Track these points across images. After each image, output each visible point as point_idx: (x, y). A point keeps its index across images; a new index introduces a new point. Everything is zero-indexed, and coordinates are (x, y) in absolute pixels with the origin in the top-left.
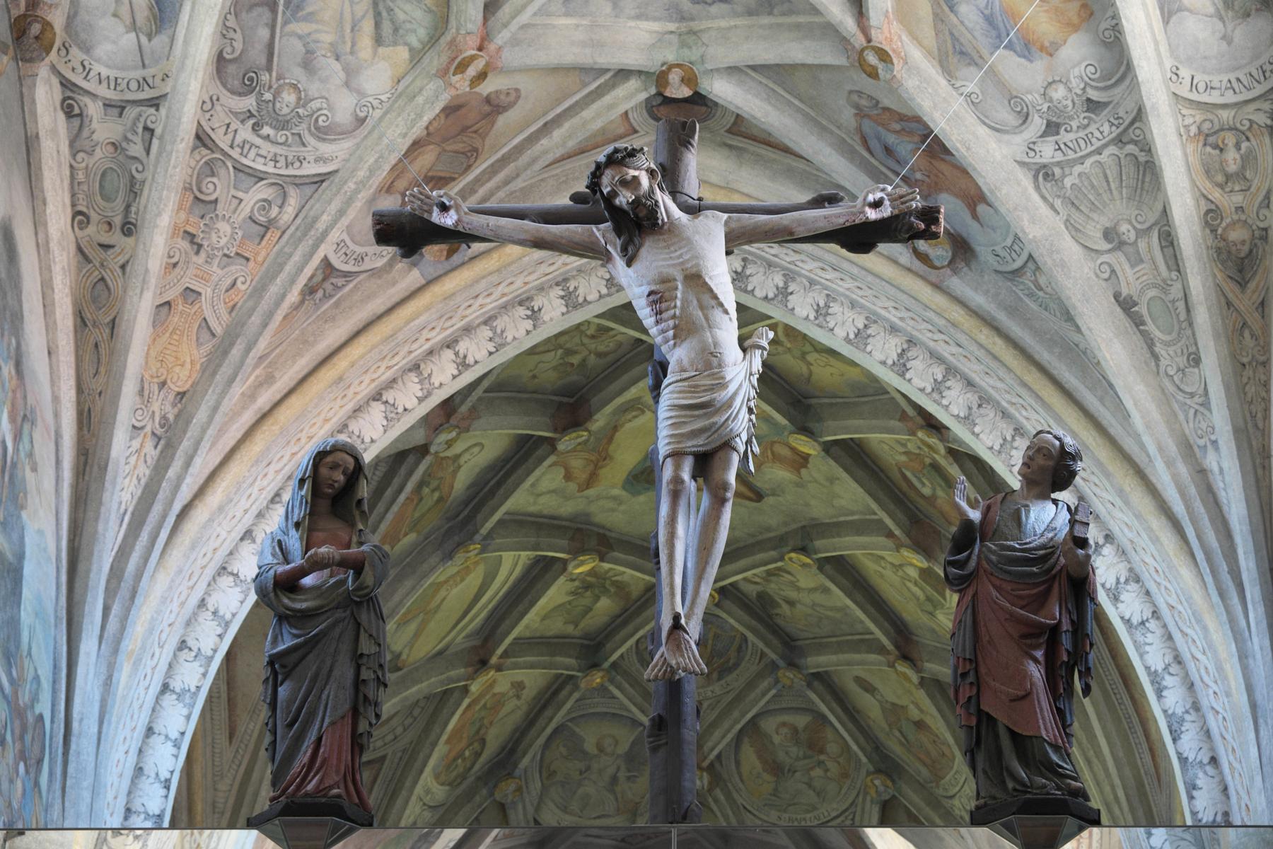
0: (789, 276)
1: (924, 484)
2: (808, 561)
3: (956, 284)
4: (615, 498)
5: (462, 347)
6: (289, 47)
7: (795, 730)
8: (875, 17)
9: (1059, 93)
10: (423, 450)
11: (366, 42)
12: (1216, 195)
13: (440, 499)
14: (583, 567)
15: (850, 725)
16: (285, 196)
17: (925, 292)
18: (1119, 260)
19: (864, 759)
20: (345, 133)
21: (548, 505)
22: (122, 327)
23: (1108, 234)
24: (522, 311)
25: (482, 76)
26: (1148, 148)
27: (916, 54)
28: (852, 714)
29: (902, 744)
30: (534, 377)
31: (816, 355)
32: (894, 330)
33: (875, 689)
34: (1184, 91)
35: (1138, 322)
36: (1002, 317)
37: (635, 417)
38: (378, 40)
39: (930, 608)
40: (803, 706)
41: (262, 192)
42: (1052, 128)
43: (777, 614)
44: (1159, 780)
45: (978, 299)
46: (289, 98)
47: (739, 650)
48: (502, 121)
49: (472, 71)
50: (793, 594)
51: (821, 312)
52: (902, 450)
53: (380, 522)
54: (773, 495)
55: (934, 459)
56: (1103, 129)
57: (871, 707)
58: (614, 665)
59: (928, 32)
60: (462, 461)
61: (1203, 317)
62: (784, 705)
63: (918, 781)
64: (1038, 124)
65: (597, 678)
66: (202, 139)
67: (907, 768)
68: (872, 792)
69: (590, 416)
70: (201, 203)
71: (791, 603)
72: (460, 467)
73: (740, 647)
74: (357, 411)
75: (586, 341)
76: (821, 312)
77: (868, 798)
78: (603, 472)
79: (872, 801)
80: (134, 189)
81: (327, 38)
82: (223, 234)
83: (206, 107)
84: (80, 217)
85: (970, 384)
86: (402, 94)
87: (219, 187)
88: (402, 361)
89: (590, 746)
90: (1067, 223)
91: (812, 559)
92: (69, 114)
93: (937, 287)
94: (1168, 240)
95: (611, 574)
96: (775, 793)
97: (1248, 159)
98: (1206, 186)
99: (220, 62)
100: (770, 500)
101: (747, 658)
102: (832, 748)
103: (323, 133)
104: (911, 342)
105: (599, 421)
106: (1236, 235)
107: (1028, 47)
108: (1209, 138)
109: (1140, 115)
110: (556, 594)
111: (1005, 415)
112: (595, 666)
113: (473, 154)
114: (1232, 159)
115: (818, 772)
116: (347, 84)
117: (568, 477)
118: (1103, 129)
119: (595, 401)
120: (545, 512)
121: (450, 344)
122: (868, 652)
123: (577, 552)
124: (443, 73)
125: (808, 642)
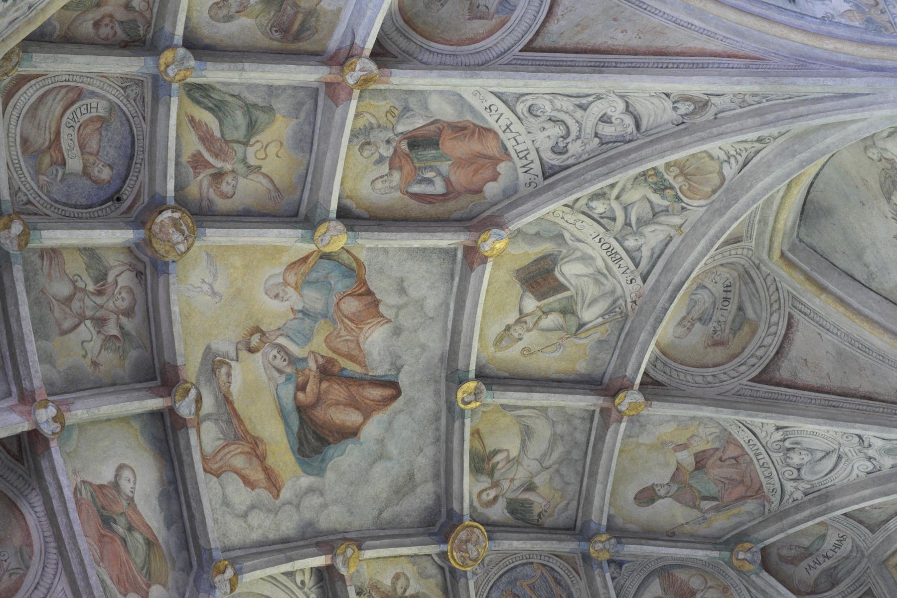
1: (430, 181)
2: (471, 385)
4: (311, 490)
13: (151, 543)
15: (680, 544)
19: (716, 554)
29: (717, 509)
30: (95, 364)
31: (250, 151)
33: (652, 488)
37: (229, 375)
39: (573, 322)
40: (643, 577)
43: (539, 515)
44: (759, 59)
47: (558, 583)
50: (521, 475)
52: (385, 168)
53: (71, 528)
54: (399, 370)
55: (406, 136)
60: (126, 487)
62: (633, 591)
63: (760, 522)
67: (744, 527)
68: (748, 567)
71: (530, 487)
72: (132, 499)
73: (555, 579)
75: (99, 300)
77: (753, 577)
78: (270, 461)
79: (757, 575)
91: (471, 380)
95: (400, 591)
100: (403, 380)
101: (569, 581)
117: (248, 483)
119: (167, 357)
120: (271, 536)
122: (604, 442)
125: (580, 514)
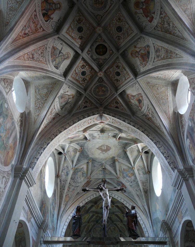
0: (112, 193)
3: (125, 194)
5: (88, 198)
6: (76, 177)
7: (113, 228)
8: (118, 175)
9: (132, 180)
10: (85, 206)
11: (82, 177)
12: (144, 187)
14: (96, 215)
16: (75, 187)
17: (122, 194)
18: (137, 192)
20: (80, 183)
21: (94, 210)
22: (63, 197)
23: (136, 190)
24: (92, 196)
25: (90, 179)
26: (138, 184)
27: (121, 178)
28: (118, 227)
32: (120, 197)
34: (141, 180)
35: (139, 196)
36: (128, 196)
38: (82, 176)
41: (73, 187)
42: (131, 182)
45: (126, 195)
46: (76, 181)
48: (91, 182)
49: (89, 179)
51: (115, 196)
56: (135, 182)
57: (119, 226)
58: (99, 223)
59: (122, 176)
61: (143, 196)
64: (130, 182)
65: (98, 224)
66: (70, 183)
69: (97, 203)
70: (69, 188)
74: (80, 203)
76: (115, 196)
80: (64, 187)
81: (79, 176)
82: (71, 190)
83: (70, 181)
84: (60, 189)
85: (126, 201)
86: (84, 180)
87: (70, 187)
88: (83, 199)
89: (97, 230)
90: (133, 189)
92: (60, 182)
93: (123, 194)
94: (140, 190)
96: (112, 234)
97: (146, 184)
98: (143, 186)
99: (71, 178)
102: (116, 230)
103: (78, 183)
104: (121, 198)
105: (98, 204)
106: (145, 190)
107: (129, 177)
108: (143, 183)
109: (138, 181)
110: (94, 217)
111: (129, 203)
112: (97, 223)
113: (89, 184)
114: (145, 185)
115: (115, 232)
116: (80, 179)
118: (135, 182)
121: (87, 198)
123: (96, 214)
124: (87, 179)
